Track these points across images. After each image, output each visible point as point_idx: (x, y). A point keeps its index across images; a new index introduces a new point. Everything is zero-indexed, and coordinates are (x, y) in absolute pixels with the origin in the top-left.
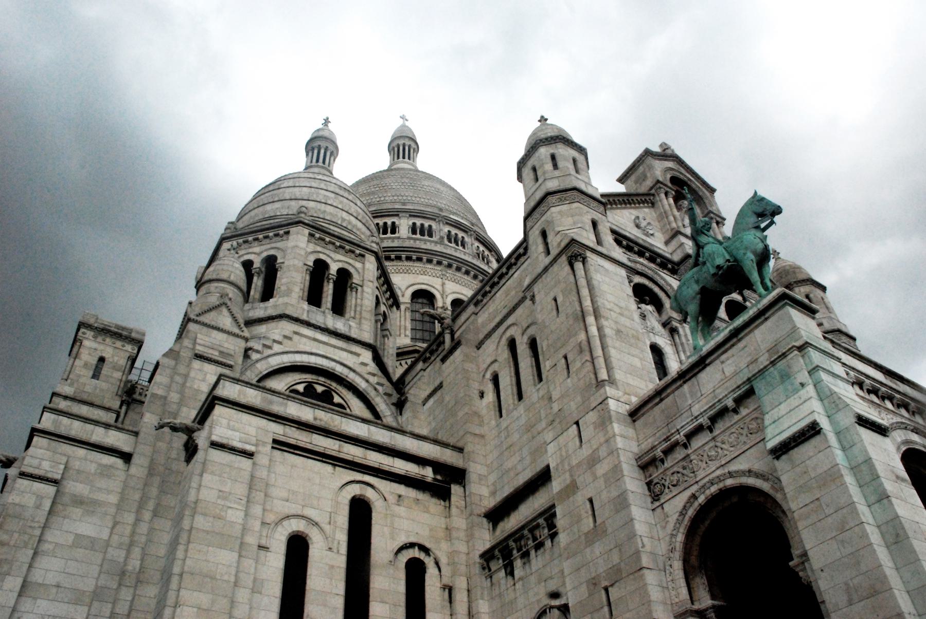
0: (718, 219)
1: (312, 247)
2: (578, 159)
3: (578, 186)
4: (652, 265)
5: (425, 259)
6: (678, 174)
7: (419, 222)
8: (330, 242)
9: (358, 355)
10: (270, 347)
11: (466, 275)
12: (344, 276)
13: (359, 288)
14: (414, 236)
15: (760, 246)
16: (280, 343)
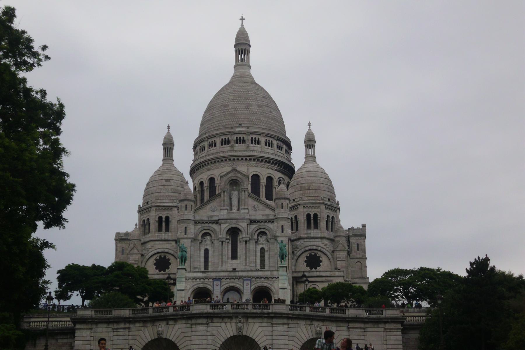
0: (244, 190)
1: (157, 213)
2: (187, 204)
3: (182, 218)
4: (210, 224)
5: (224, 160)
6: (232, 177)
7: (223, 137)
8: (162, 209)
9: (171, 244)
10: (148, 251)
11: (242, 160)
12: (167, 218)
13: (171, 221)
14: (222, 146)
15: (181, 256)
16: (151, 249)
